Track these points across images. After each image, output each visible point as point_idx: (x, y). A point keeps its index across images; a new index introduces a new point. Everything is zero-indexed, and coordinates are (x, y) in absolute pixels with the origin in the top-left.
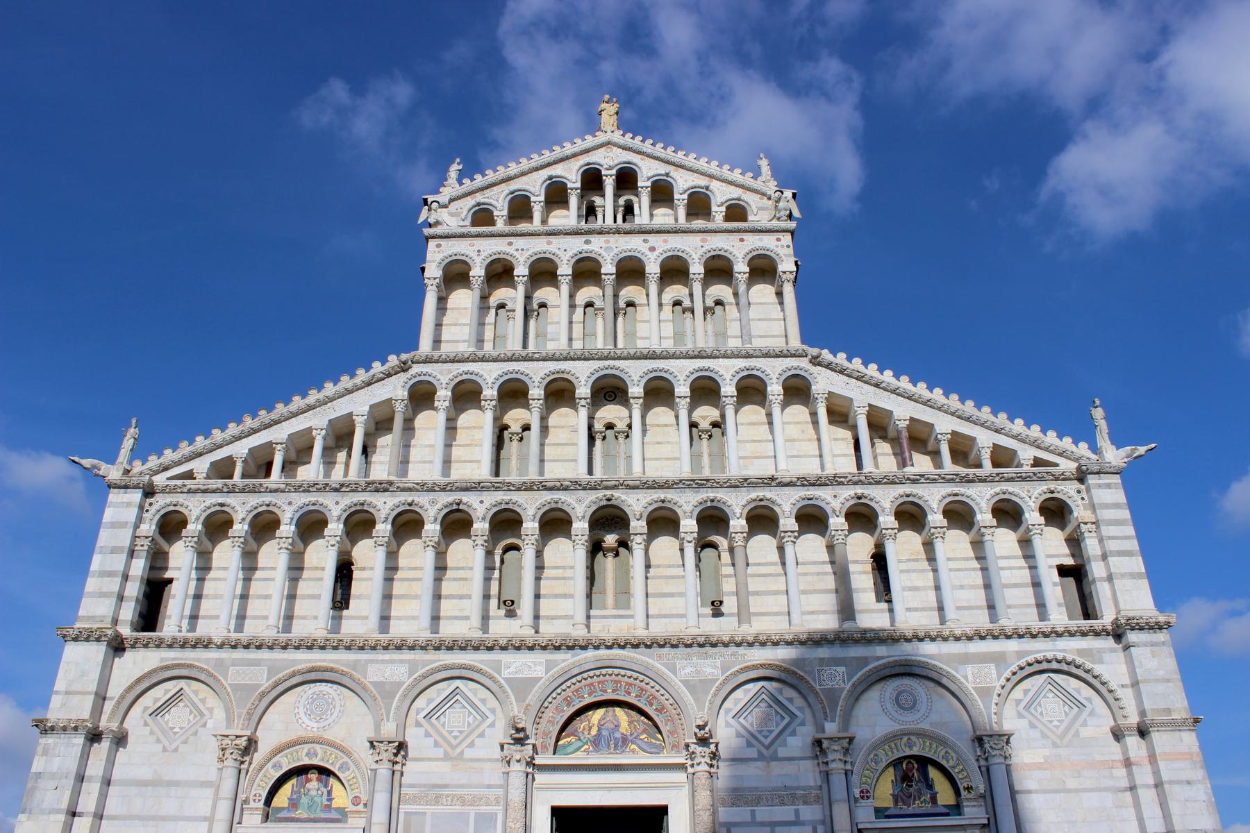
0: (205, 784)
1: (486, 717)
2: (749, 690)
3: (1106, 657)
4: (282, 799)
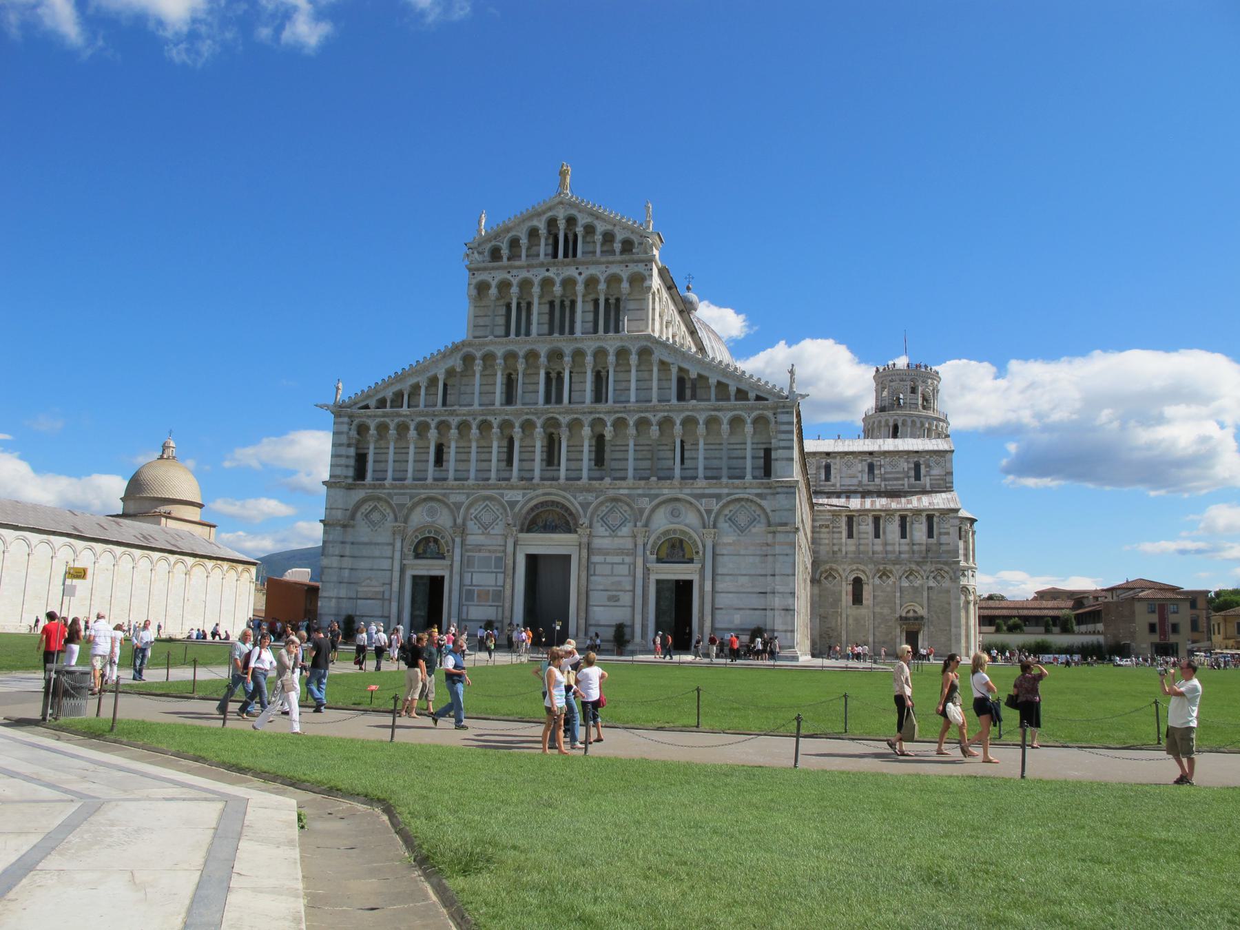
3: (768, 497)
4: (420, 551)
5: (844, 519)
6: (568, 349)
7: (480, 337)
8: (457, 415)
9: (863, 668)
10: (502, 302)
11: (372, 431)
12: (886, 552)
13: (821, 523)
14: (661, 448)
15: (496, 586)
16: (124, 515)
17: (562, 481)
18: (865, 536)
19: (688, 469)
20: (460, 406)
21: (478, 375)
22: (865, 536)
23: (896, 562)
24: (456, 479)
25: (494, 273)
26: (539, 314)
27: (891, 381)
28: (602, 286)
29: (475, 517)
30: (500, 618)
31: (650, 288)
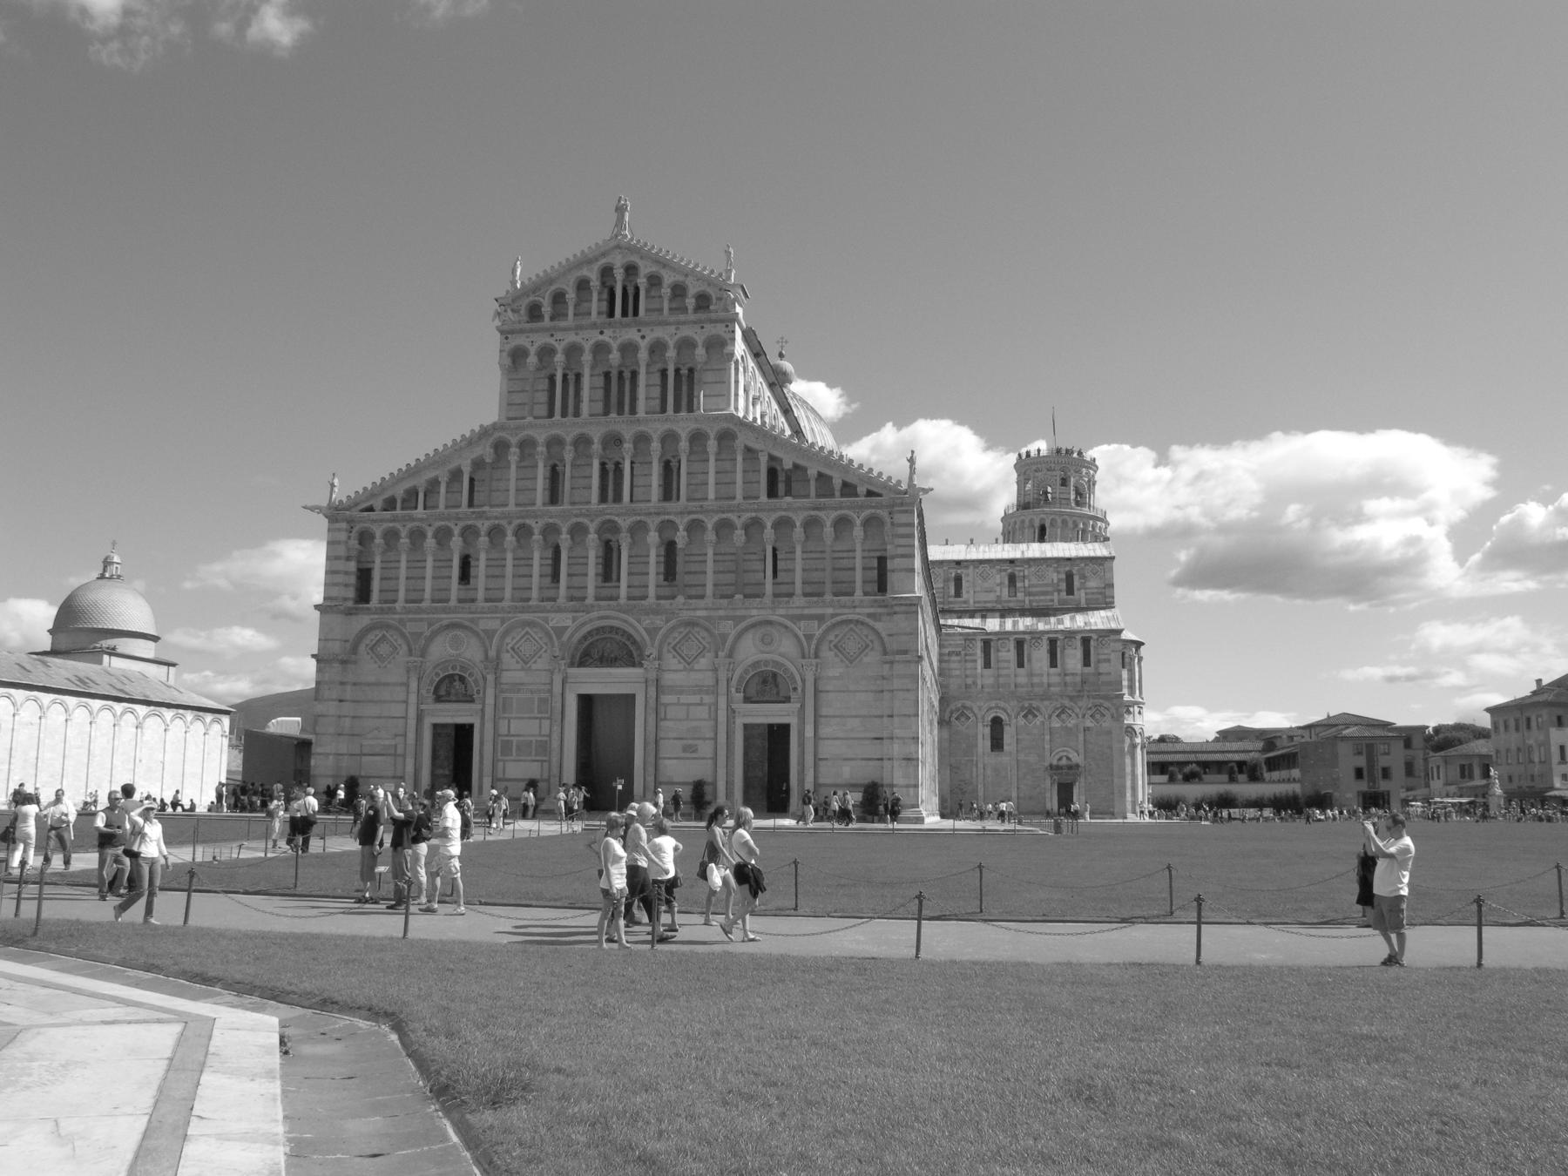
0: (402, 684)
1: (542, 648)
2: (681, 633)
4: (442, 692)
5: (979, 645)
6: (628, 433)
7: (516, 419)
8: (487, 519)
9: (1005, 831)
10: (544, 373)
11: (379, 540)
12: (1032, 685)
13: (951, 649)
14: (747, 557)
15: (540, 735)
16: (54, 652)
17: (623, 600)
18: (1006, 665)
19: (782, 583)
20: (491, 506)
21: (513, 467)
22: (1006, 665)
23: (1045, 697)
24: (487, 600)
25: (534, 337)
26: (591, 388)
27: (1036, 471)
28: (671, 353)
29: (513, 649)
30: (545, 776)
31: (732, 354)
